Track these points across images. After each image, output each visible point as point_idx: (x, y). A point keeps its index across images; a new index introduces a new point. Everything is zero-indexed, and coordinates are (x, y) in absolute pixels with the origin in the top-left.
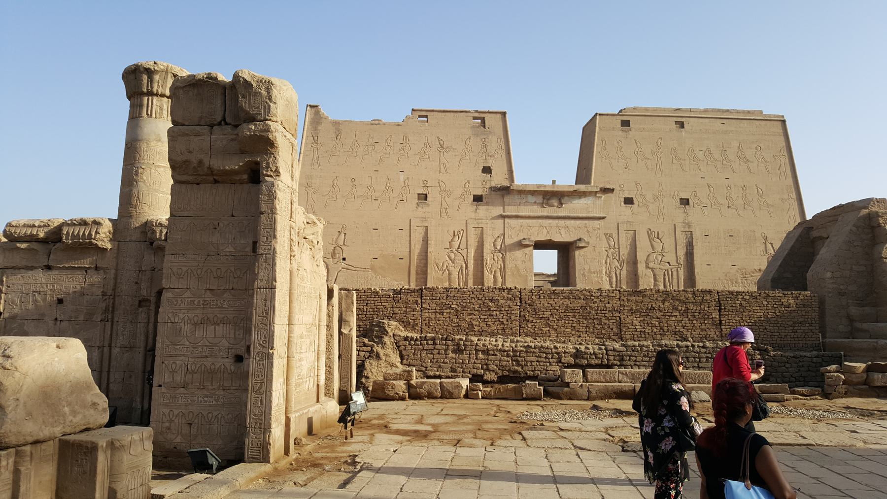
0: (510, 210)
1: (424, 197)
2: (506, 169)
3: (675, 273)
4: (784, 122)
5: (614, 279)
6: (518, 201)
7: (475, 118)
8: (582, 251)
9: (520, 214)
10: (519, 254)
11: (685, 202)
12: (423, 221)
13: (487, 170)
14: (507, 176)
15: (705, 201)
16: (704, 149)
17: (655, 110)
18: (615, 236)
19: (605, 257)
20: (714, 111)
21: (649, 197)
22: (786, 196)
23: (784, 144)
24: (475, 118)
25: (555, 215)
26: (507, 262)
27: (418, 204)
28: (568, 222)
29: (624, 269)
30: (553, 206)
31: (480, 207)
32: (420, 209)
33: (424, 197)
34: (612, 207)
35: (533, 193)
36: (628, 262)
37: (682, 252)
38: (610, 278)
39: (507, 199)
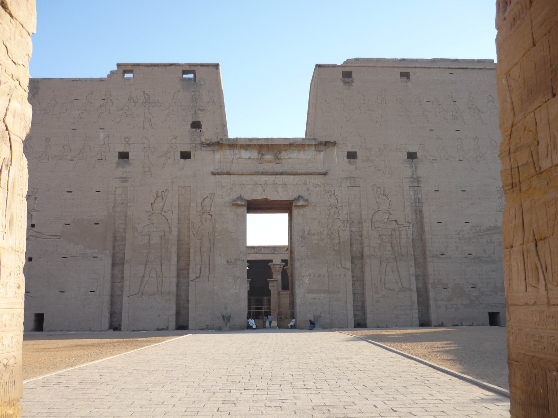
1: (124, 156)
8: (302, 211)
11: (412, 156)
12: (122, 181)
13: (196, 125)
24: (185, 72)
27: (118, 164)
28: (285, 178)
32: (120, 169)
33: (124, 156)
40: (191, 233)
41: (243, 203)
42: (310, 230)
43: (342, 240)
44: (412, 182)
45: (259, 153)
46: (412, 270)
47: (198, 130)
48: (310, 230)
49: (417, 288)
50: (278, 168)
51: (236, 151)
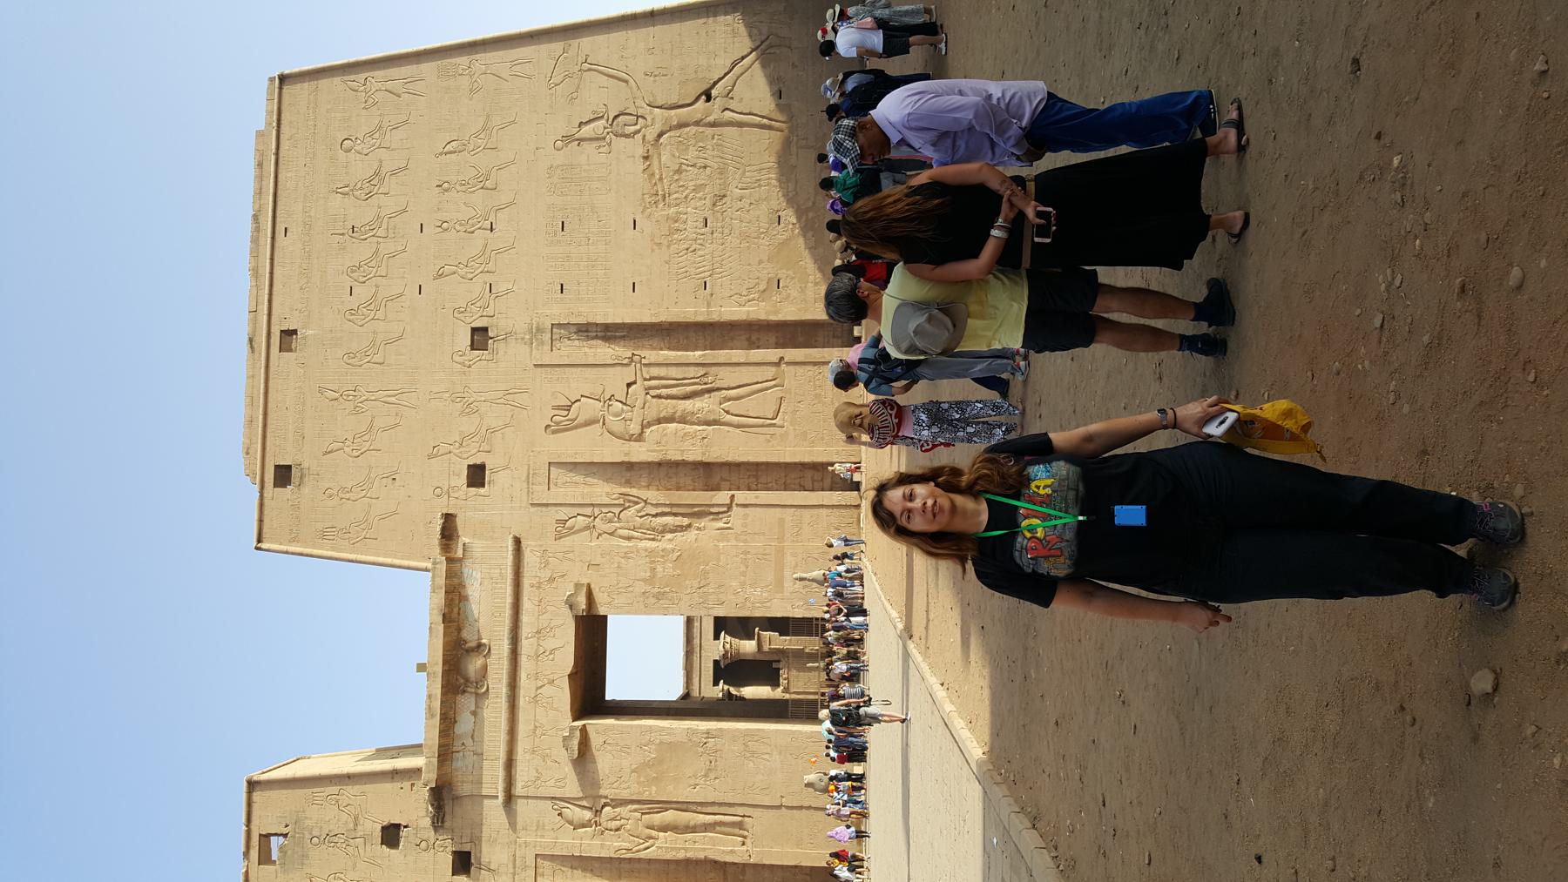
0: (493, 778)
2: (388, 787)
3: (655, 371)
4: (283, 79)
5: (669, 520)
6: (471, 758)
7: (265, 858)
8: (600, 598)
9: (502, 756)
10: (604, 762)
11: (480, 337)
13: (391, 834)
14: (407, 785)
15: (478, 287)
16: (348, 282)
17: (252, 402)
18: (563, 513)
19: (615, 541)
20: (255, 254)
21: (468, 425)
22: (465, 82)
23: (337, 80)
25: (505, 664)
26: (625, 795)
28: (526, 631)
29: (644, 494)
30: (485, 668)
31: (484, 860)
34: (489, 520)
35: (448, 722)
36: (628, 483)
37: (605, 351)
38: (665, 530)
39: (464, 789)
40: (642, 855)
41: (578, 733)
42: (644, 580)
43: (667, 510)
44: (543, 343)
45: (464, 691)
46: (737, 355)
47: (404, 833)
48: (644, 580)
49: (778, 346)
50: (502, 648)
51: (457, 746)
